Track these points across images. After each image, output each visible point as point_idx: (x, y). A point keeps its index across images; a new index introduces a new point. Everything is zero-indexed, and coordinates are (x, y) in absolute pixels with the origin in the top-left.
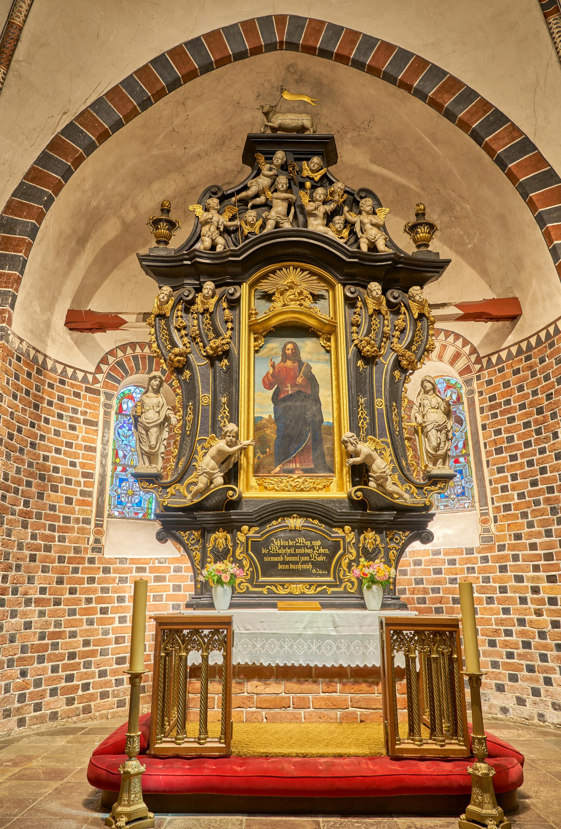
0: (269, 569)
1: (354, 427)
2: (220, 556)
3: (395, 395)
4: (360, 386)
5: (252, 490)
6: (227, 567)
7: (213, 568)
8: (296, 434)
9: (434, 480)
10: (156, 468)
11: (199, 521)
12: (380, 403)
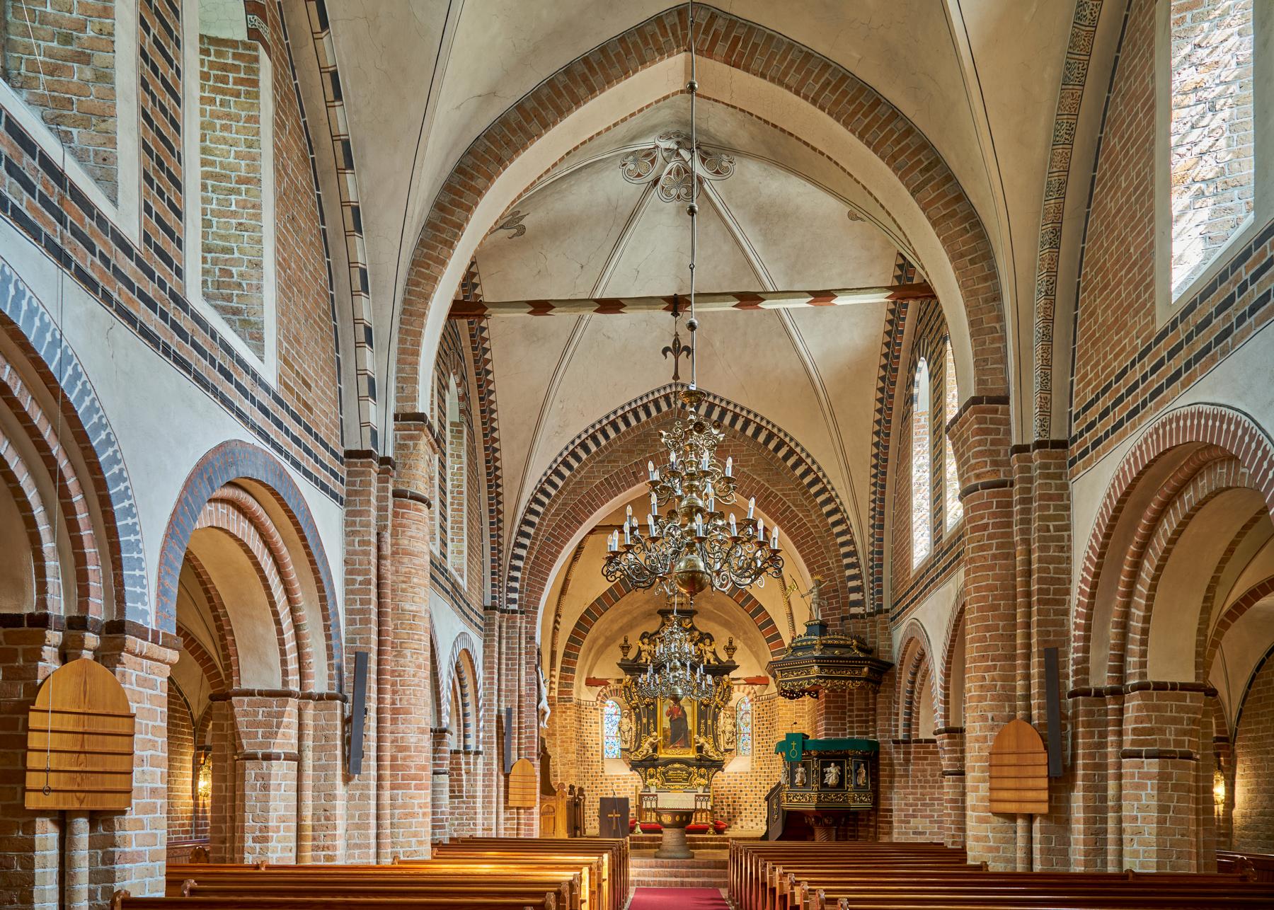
0: (668, 781)
1: (699, 733)
2: (652, 777)
3: (716, 718)
4: (702, 715)
5: (663, 754)
6: (654, 781)
7: (649, 781)
8: (678, 734)
9: (726, 750)
10: (627, 746)
11: (644, 765)
12: (709, 722)
